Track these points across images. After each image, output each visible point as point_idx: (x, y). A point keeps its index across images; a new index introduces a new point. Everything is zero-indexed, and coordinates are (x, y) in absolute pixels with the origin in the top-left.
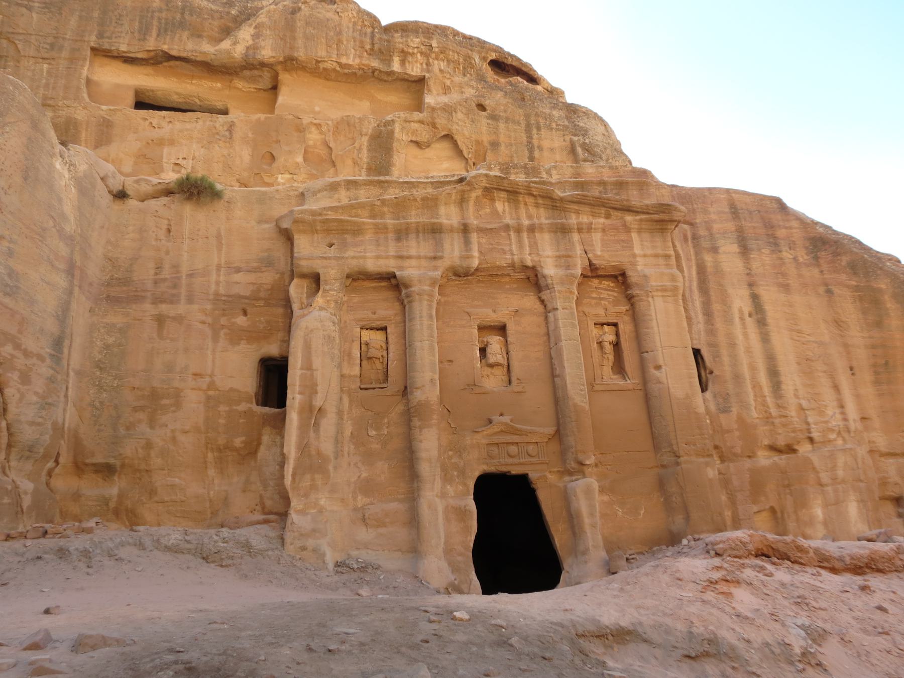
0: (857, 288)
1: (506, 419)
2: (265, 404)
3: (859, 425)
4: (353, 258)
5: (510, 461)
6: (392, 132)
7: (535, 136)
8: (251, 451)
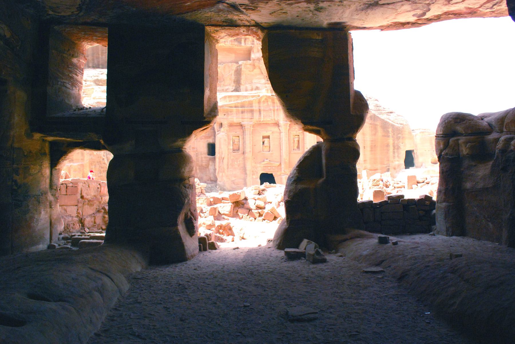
0: (371, 124)
1: (268, 160)
2: (209, 155)
3: (363, 162)
6: (241, 69)
8: (207, 166)
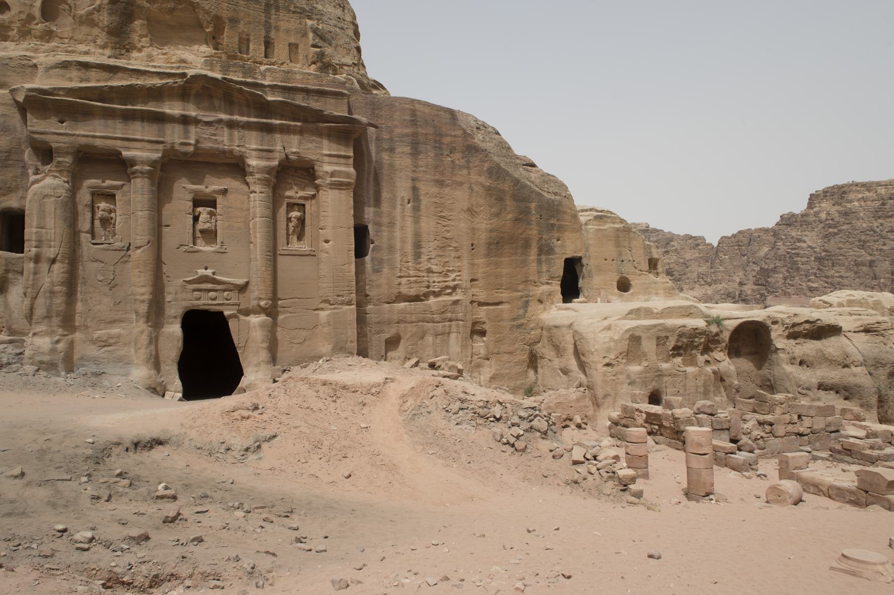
4: (84, 136)
5: (210, 302)
7: (273, 17)
